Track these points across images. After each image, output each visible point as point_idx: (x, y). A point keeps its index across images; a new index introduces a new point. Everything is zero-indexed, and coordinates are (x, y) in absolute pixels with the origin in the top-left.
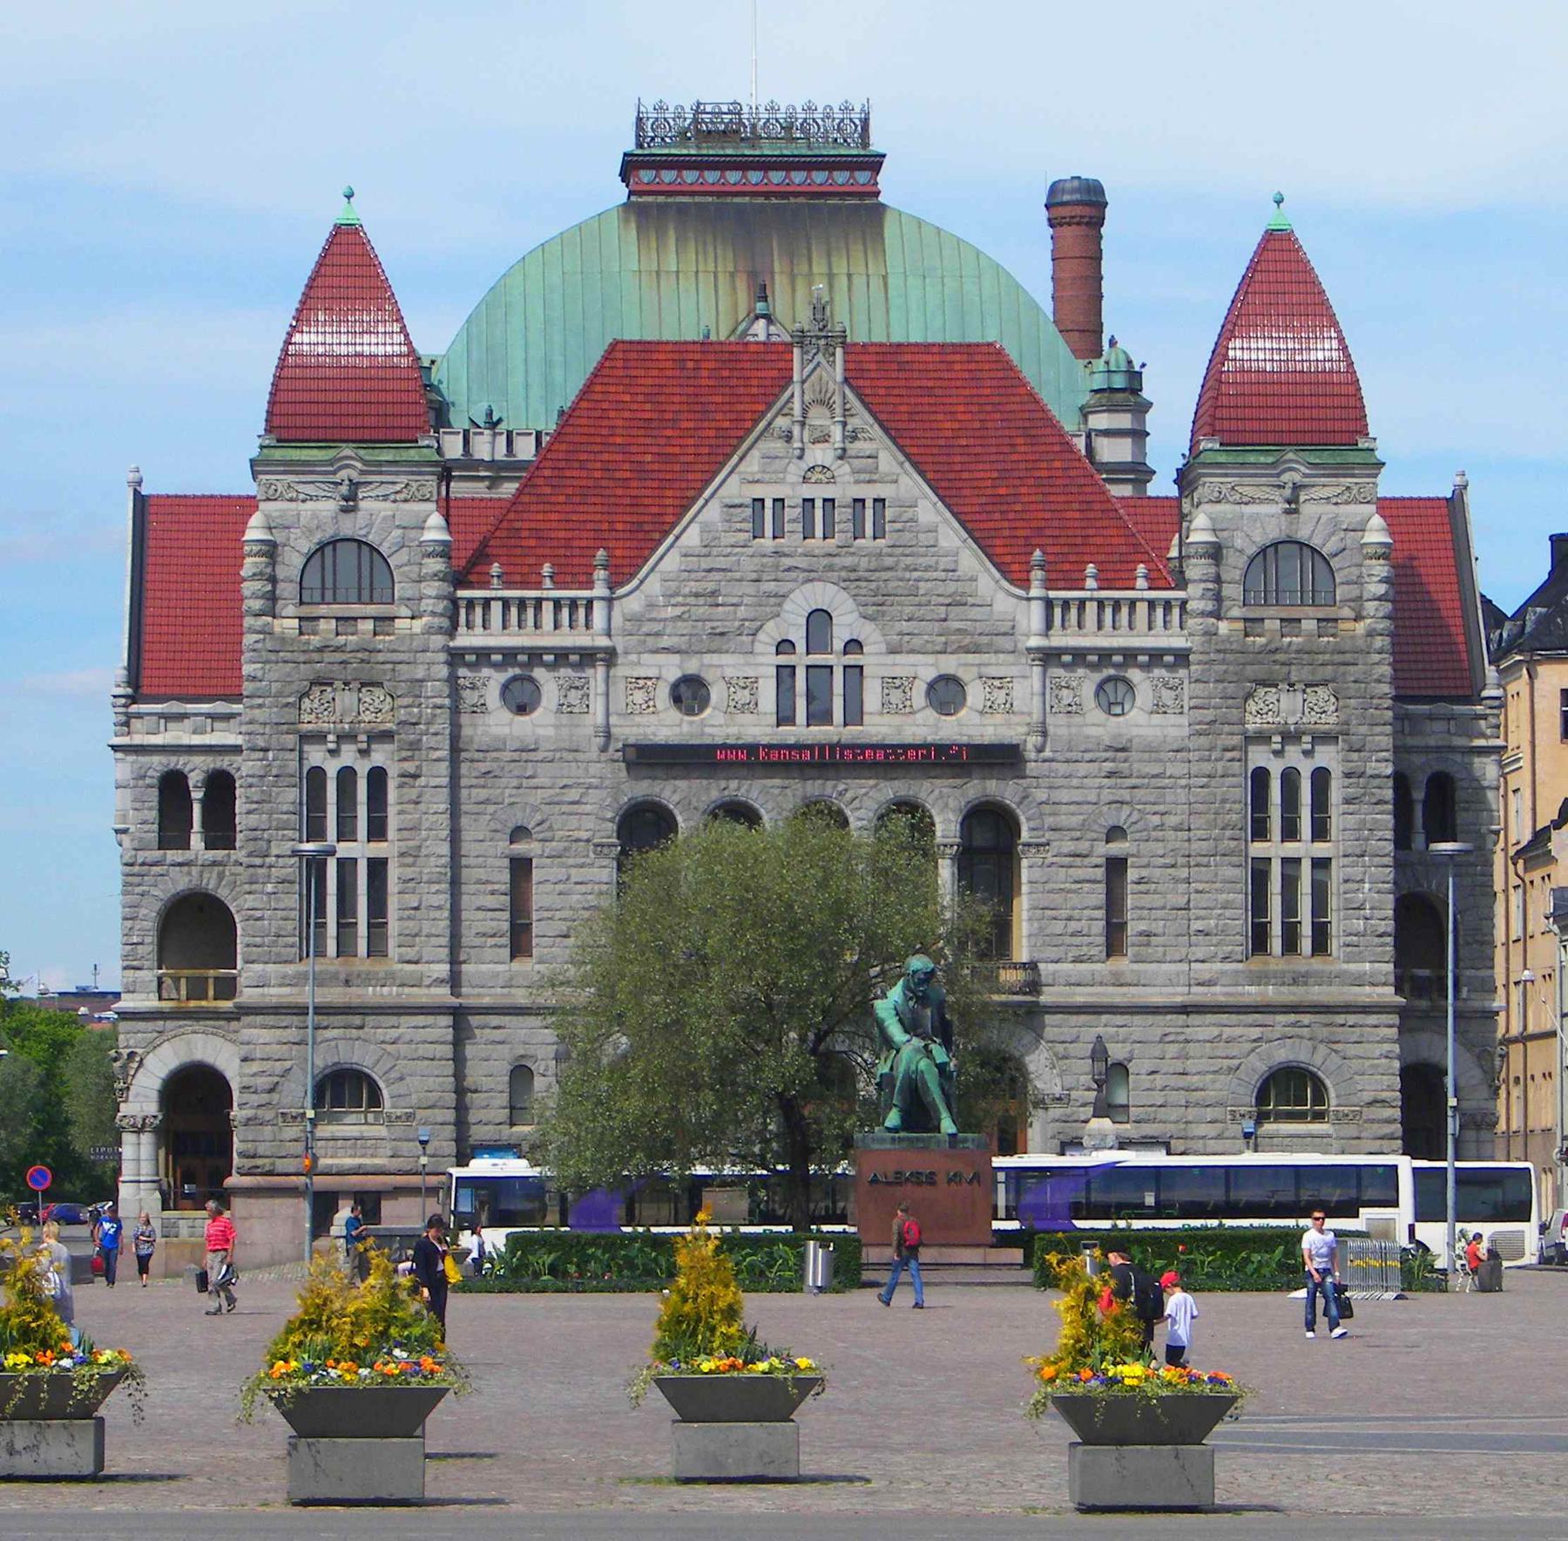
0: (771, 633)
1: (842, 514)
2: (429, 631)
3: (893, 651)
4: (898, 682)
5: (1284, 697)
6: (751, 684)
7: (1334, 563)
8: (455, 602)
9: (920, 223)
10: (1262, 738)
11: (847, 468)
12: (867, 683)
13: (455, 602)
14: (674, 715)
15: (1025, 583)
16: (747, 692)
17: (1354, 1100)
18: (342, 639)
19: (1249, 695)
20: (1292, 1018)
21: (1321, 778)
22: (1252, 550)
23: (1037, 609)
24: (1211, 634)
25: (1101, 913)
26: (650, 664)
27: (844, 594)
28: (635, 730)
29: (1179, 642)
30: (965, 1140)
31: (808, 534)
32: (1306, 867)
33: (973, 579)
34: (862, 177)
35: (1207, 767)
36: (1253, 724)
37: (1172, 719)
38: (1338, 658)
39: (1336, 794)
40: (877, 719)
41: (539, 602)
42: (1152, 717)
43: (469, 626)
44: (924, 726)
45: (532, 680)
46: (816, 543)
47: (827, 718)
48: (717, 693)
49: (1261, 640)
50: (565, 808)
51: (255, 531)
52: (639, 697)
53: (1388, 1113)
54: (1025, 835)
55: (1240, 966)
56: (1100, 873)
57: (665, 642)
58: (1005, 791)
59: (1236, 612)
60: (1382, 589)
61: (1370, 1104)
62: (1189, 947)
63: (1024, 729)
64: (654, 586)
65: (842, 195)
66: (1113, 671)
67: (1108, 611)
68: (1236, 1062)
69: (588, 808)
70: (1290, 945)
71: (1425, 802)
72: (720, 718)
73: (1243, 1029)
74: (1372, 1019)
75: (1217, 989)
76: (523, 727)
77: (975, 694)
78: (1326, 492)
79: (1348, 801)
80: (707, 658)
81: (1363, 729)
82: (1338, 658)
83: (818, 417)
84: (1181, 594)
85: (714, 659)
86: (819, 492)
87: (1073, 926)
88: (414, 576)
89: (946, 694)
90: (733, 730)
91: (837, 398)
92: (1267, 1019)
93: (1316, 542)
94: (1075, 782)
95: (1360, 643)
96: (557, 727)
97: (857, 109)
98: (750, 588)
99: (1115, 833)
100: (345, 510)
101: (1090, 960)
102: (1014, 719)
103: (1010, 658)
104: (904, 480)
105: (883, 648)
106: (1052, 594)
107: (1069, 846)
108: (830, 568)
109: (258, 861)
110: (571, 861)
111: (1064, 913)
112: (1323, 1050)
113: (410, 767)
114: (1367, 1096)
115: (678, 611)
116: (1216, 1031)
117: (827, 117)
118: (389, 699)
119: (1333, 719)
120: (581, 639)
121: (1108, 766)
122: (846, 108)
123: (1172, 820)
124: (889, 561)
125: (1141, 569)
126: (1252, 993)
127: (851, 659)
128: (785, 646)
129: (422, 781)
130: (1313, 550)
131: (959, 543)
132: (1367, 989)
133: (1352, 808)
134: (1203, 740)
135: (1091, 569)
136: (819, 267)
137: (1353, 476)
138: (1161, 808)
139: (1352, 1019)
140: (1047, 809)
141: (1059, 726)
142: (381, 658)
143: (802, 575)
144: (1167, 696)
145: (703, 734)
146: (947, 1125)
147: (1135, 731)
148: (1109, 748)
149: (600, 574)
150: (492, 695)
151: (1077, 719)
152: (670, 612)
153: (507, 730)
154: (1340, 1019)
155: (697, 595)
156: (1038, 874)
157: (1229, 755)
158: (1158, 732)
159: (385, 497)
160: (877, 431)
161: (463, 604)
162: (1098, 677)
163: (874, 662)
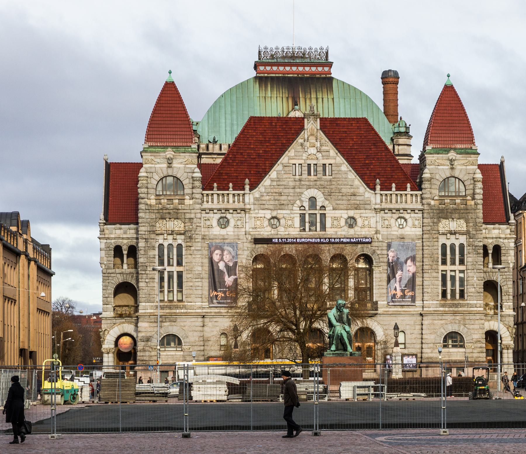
1: (320, 169)
2: (195, 203)
6: (292, 219)
7: (466, 183)
8: (203, 194)
9: (343, 83)
11: (320, 155)
13: (203, 194)
15: (374, 189)
16: (291, 221)
18: (169, 206)
22: (441, 180)
24: (429, 204)
26: (262, 213)
29: (420, 207)
31: (309, 174)
34: (326, 69)
40: (330, 230)
43: (208, 202)
45: (226, 217)
46: (312, 177)
48: (282, 221)
51: (142, 173)
52: (258, 223)
55: (438, 302)
57: (267, 206)
59: (436, 198)
65: (320, 74)
67: (399, 197)
69: (243, 256)
76: (223, 232)
77: (359, 221)
78: (463, 162)
80: (279, 211)
83: (312, 140)
84: (420, 192)
85: (281, 212)
86: (312, 162)
88: (191, 187)
89: (351, 222)
90: (287, 233)
93: (460, 177)
95: (473, 207)
96: (234, 232)
97: (325, 49)
98: (291, 191)
103: (369, 211)
104: (338, 158)
105: (332, 208)
109: (144, 272)
112: (462, 327)
113: (188, 244)
117: (316, 51)
118: (183, 224)
119: (465, 229)
120: (241, 205)
122: (321, 49)
129: (192, 248)
130: (459, 179)
131: (354, 177)
136: (313, 96)
137: (471, 157)
140: (380, 256)
141: (384, 231)
142: (180, 211)
144: (417, 223)
147: (407, 233)
149: (247, 187)
150: (215, 223)
151: (389, 229)
152: (267, 198)
153: (218, 233)
158: (413, 233)
159: (181, 163)
160: (330, 144)
161: (205, 195)
163: (330, 213)
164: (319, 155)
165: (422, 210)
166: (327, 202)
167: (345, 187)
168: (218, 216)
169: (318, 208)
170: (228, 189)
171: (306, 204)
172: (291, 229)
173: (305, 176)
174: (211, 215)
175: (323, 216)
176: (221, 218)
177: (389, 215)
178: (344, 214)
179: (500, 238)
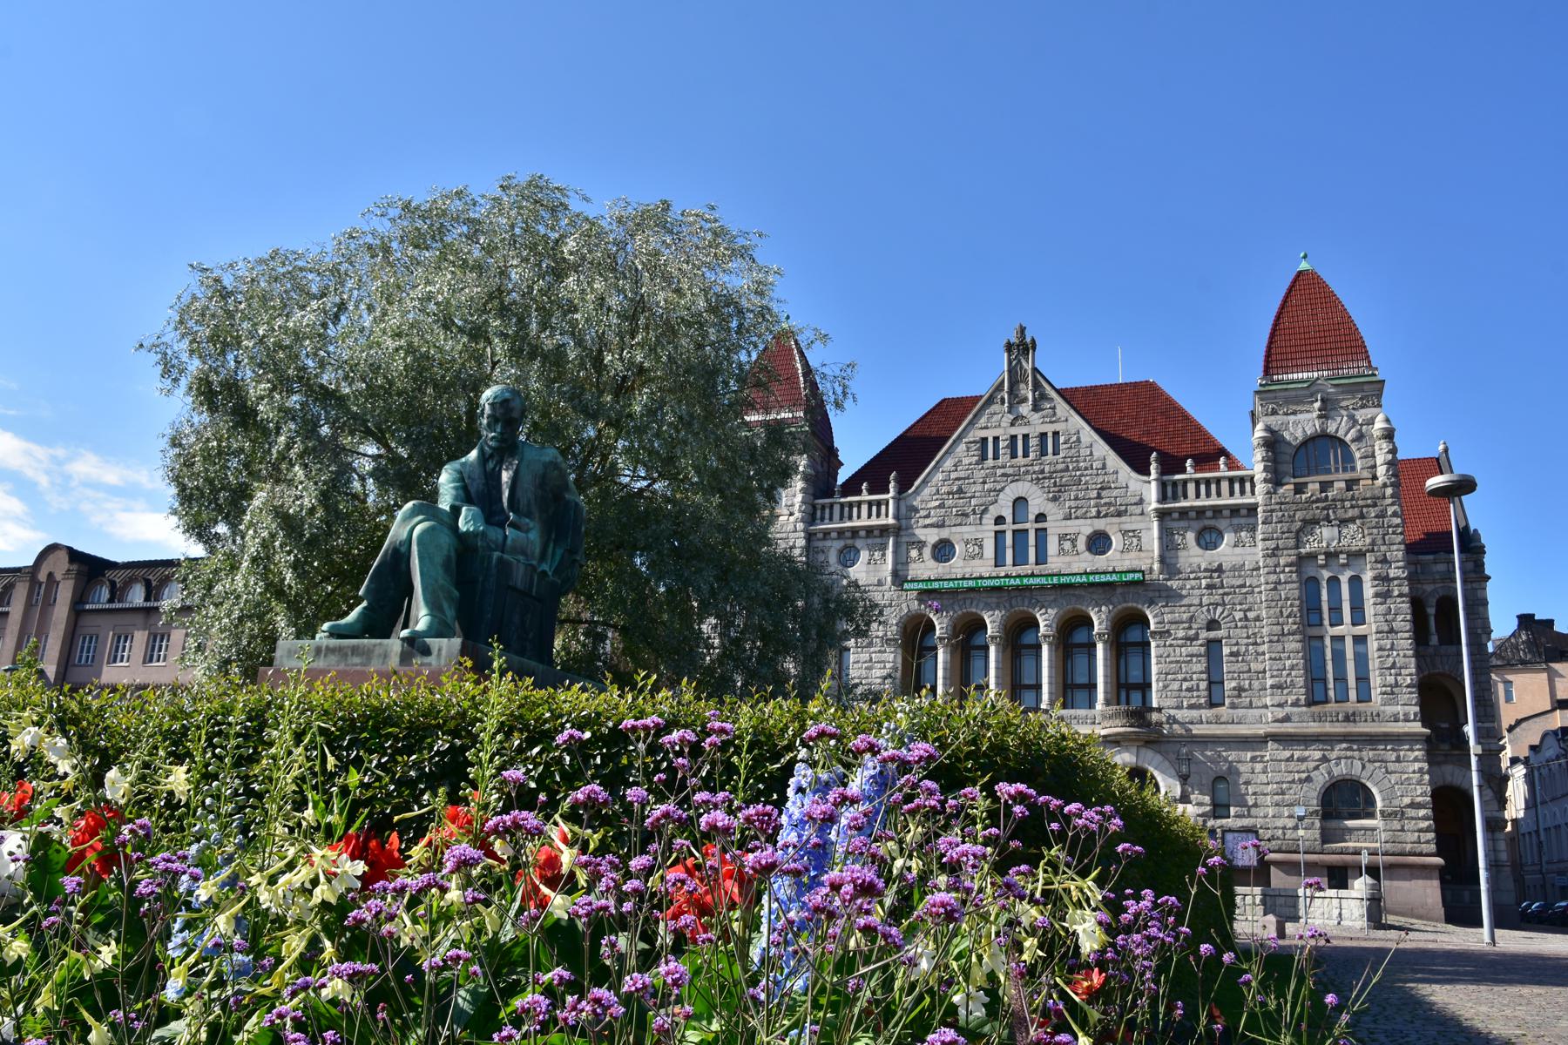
0: (994, 512)
1: (1033, 442)
3: (1068, 517)
8: (814, 507)
10: (1312, 556)
12: (1049, 538)
13: (814, 507)
21: (1356, 582)
25: (1204, 676)
31: (1014, 455)
32: (1349, 642)
35: (1273, 578)
36: (1307, 549)
37: (1248, 550)
39: (1369, 591)
40: (1055, 559)
46: (1020, 460)
54: (1152, 627)
56: (1203, 649)
57: (928, 521)
71: (1436, 616)
72: (961, 563)
77: (1116, 541)
79: (1377, 595)
81: (1383, 548)
85: (958, 529)
86: (1019, 431)
87: (1185, 685)
89: (1099, 542)
90: (968, 570)
93: (1340, 434)
98: (979, 487)
99: (1212, 625)
107: (1181, 634)
108: (1027, 472)
111: (1180, 677)
114: (1407, 800)
120: (882, 521)
126: (1314, 728)
128: (1000, 520)
147: (1223, 559)
148: (1206, 570)
149: (892, 485)
156: (1161, 650)
163: (1054, 527)
165: (1252, 509)
166: (1051, 505)
168: (839, 544)
170: (859, 493)
171: (1007, 514)
172: (977, 562)
173: (1004, 458)
174: (828, 543)
175: (1041, 534)
176: (846, 547)
177: (1183, 524)
178: (1086, 528)
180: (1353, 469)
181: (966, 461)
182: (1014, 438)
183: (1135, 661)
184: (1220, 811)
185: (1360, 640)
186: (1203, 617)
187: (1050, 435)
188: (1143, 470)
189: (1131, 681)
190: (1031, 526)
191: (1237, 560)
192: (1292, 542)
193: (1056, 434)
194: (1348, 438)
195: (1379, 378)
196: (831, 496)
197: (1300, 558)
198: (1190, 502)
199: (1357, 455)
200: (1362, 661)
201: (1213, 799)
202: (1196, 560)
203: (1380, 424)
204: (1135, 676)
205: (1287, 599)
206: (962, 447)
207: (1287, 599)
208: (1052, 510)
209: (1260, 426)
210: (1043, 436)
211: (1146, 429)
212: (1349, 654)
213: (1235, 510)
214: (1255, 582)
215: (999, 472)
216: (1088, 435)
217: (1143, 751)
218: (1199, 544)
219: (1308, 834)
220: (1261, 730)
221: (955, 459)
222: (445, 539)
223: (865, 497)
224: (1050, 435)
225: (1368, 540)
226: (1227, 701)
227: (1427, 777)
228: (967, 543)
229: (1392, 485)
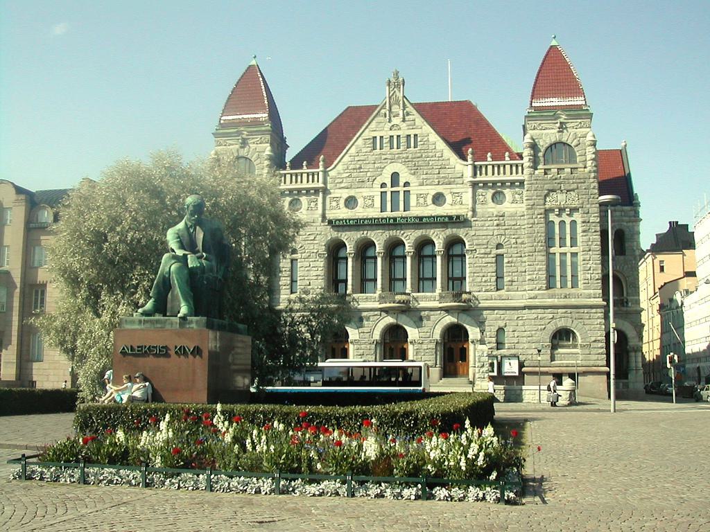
1: (403, 140)
3: (422, 184)
4: (422, 196)
5: (559, 195)
6: (372, 198)
10: (552, 210)
12: (411, 196)
14: (345, 210)
17: (588, 340)
19: (546, 196)
20: (564, 310)
21: (573, 223)
23: (470, 168)
25: (494, 274)
27: (404, 167)
28: (333, 215)
29: (519, 177)
30: (191, 322)
31: (392, 148)
33: (449, 159)
35: (532, 221)
36: (548, 206)
38: (578, 181)
39: (579, 229)
40: (415, 208)
41: (302, 174)
42: (513, 204)
44: (432, 210)
47: (398, 210)
48: (360, 201)
49: (549, 176)
50: (309, 242)
53: (600, 345)
54: (467, 247)
57: (342, 185)
58: (461, 232)
60: (594, 156)
61: (595, 341)
62: (525, 288)
63: (467, 210)
64: (340, 167)
66: (498, 191)
68: (544, 327)
70: (563, 286)
72: (361, 210)
73: (548, 314)
74: (594, 310)
75: (536, 300)
77: (449, 198)
80: (357, 190)
82: (578, 181)
87: (484, 279)
89: (438, 199)
91: (401, 102)
92: (555, 311)
93: (568, 142)
94: (485, 228)
98: (372, 166)
99: (499, 246)
100: (241, 147)
101: (491, 291)
102: (463, 207)
103: (461, 186)
106: (476, 163)
107: (483, 251)
108: (399, 158)
110: (311, 260)
111: (481, 274)
114: (593, 339)
115: (347, 175)
116: (535, 316)
121: (495, 223)
123: (519, 241)
124: (419, 155)
125: (507, 154)
126: (549, 302)
127: (406, 189)
128: (383, 185)
132: (592, 300)
133: (585, 234)
134: (530, 211)
135: (489, 154)
138: (516, 236)
139: (586, 310)
141: (479, 209)
143: (389, 161)
145: (355, 215)
146: (184, 310)
149: (321, 163)
151: (486, 206)
154: (582, 310)
155: (354, 169)
156: (472, 260)
157: (539, 216)
158: (513, 210)
159: (254, 143)
160: (414, 112)
162: (493, 191)
163: (414, 189)
164: (403, 125)
165: (522, 183)
167: (432, 159)
168: (288, 199)
169: (401, 184)
170: (301, 167)
172: (371, 210)
173: (386, 149)
175: (407, 193)
178: (432, 191)
179: (623, 221)
180: (575, 162)
181: (364, 150)
182: (392, 137)
183: (457, 264)
184: (500, 346)
185: (574, 255)
186: (495, 241)
187: (412, 136)
188: (464, 158)
189: (455, 276)
190: (401, 189)
191: (512, 210)
192: (542, 202)
193: (416, 136)
194: (572, 145)
195: (591, 112)
196: (285, 168)
197: (546, 210)
198: (490, 178)
199: (578, 154)
200: (574, 266)
201: (497, 340)
202: (491, 210)
203: (589, 137)
204: (457, 273)
205: (538, 233)
206: (360, 142)
207: (538, 233)
208: (412, 179)
209: (528, 136)
210: (408, 136)
211: (464, 130)
212: (569, 263)
213: (513, 183)
214: (522, 222)
215: (384, 157)
216: (434, 137)
217: (460, 315)
218: (493, 201)
219: (545, 357)
220: (522, 305)
221: (358, 146)
222: (186, 272)
223: (305, 170)
224: (412, 136)
225: (581, 201)
226: (505, 287)
227: (603, 327)
228: (365, 198)
229: (594, 172)
